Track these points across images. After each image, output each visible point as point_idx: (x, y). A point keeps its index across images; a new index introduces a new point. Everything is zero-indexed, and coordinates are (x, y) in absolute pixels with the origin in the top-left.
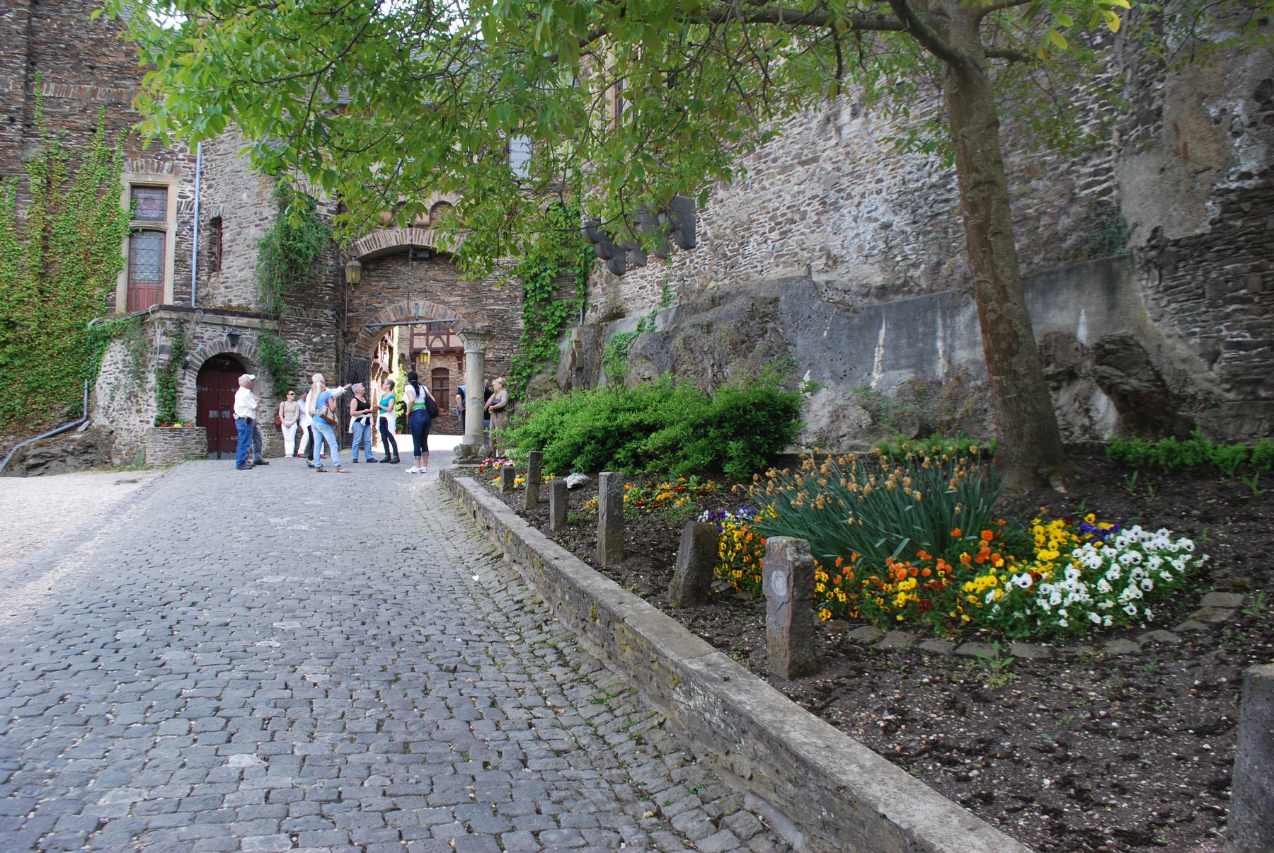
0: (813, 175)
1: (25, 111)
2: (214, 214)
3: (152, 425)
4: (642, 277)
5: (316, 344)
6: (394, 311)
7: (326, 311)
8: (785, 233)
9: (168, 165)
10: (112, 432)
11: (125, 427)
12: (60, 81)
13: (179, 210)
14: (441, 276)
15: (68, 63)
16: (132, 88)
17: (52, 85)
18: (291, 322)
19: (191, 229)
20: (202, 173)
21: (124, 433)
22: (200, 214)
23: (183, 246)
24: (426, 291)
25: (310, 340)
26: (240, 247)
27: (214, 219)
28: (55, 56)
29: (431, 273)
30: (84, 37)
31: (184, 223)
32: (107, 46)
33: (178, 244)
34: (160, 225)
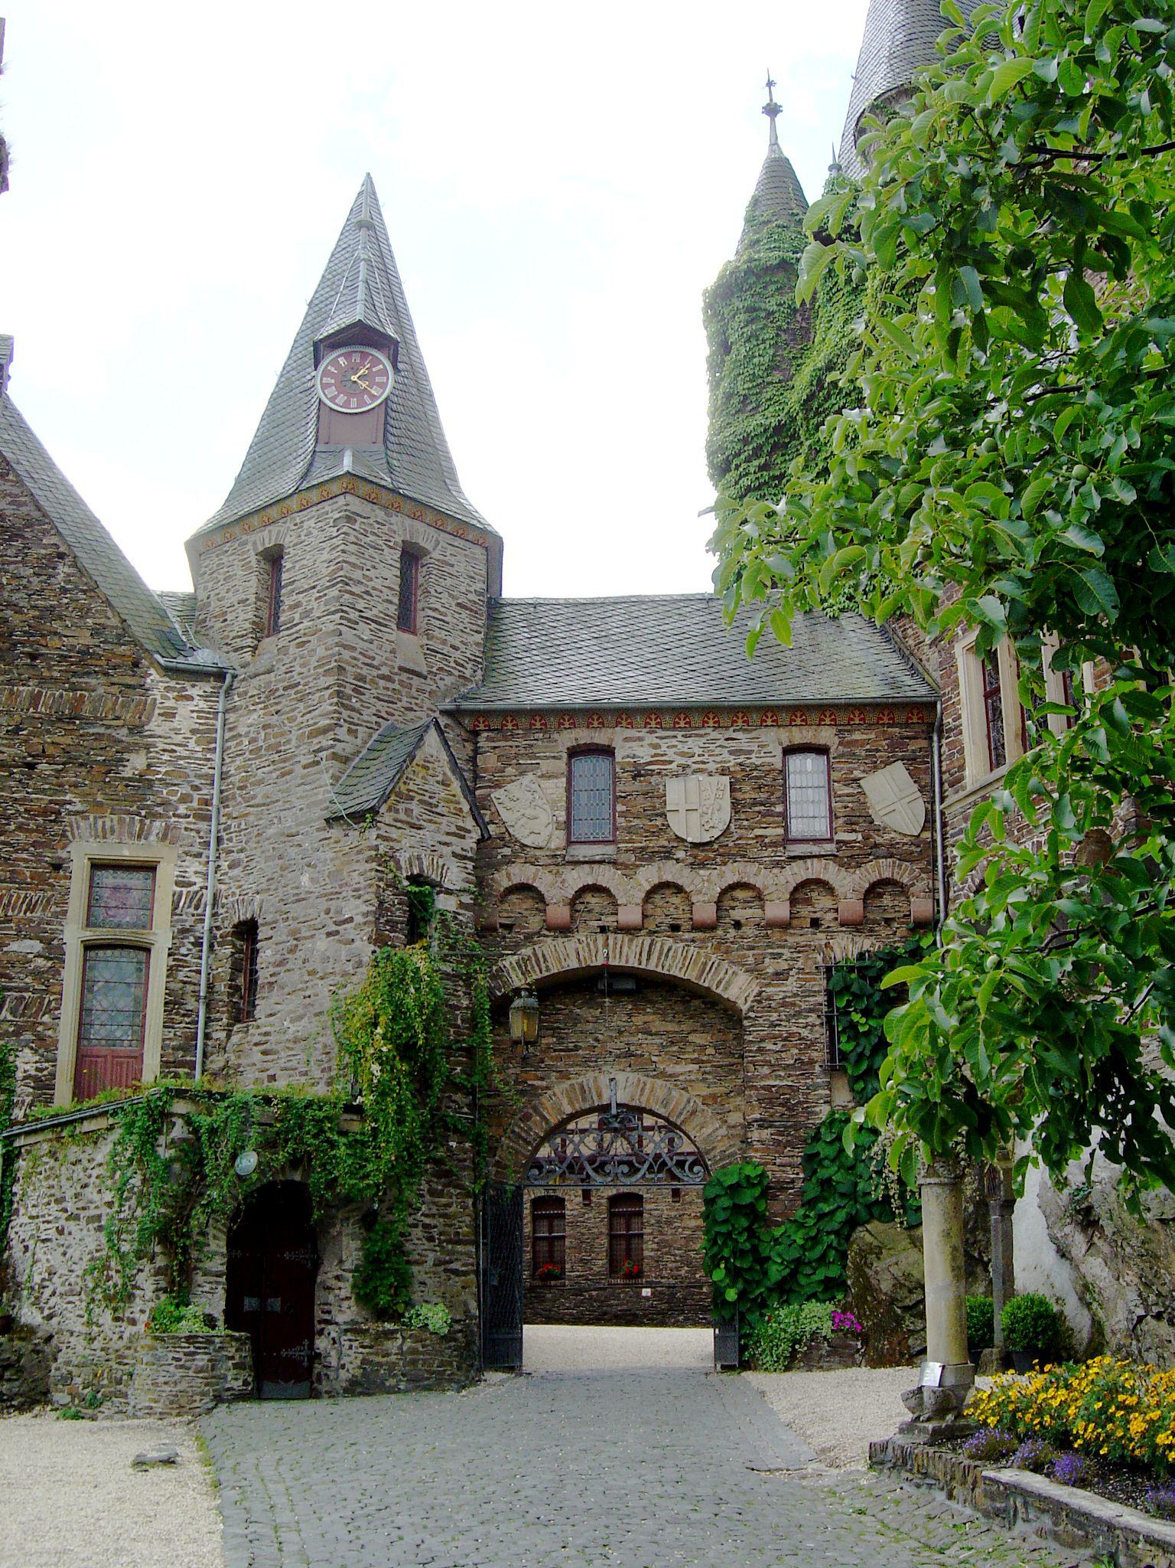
6: (570, 1094)
9: (158, 825)
14: (657, 1025)
16: (101, 690)
19: (198, 944)
20: (219, 840)
24: (629, 1054)
26: (295, 976)
27: (241, 924)
29: (639, 1020)
31: (184, 931)
32: (60, 618)
33: (171, 971)
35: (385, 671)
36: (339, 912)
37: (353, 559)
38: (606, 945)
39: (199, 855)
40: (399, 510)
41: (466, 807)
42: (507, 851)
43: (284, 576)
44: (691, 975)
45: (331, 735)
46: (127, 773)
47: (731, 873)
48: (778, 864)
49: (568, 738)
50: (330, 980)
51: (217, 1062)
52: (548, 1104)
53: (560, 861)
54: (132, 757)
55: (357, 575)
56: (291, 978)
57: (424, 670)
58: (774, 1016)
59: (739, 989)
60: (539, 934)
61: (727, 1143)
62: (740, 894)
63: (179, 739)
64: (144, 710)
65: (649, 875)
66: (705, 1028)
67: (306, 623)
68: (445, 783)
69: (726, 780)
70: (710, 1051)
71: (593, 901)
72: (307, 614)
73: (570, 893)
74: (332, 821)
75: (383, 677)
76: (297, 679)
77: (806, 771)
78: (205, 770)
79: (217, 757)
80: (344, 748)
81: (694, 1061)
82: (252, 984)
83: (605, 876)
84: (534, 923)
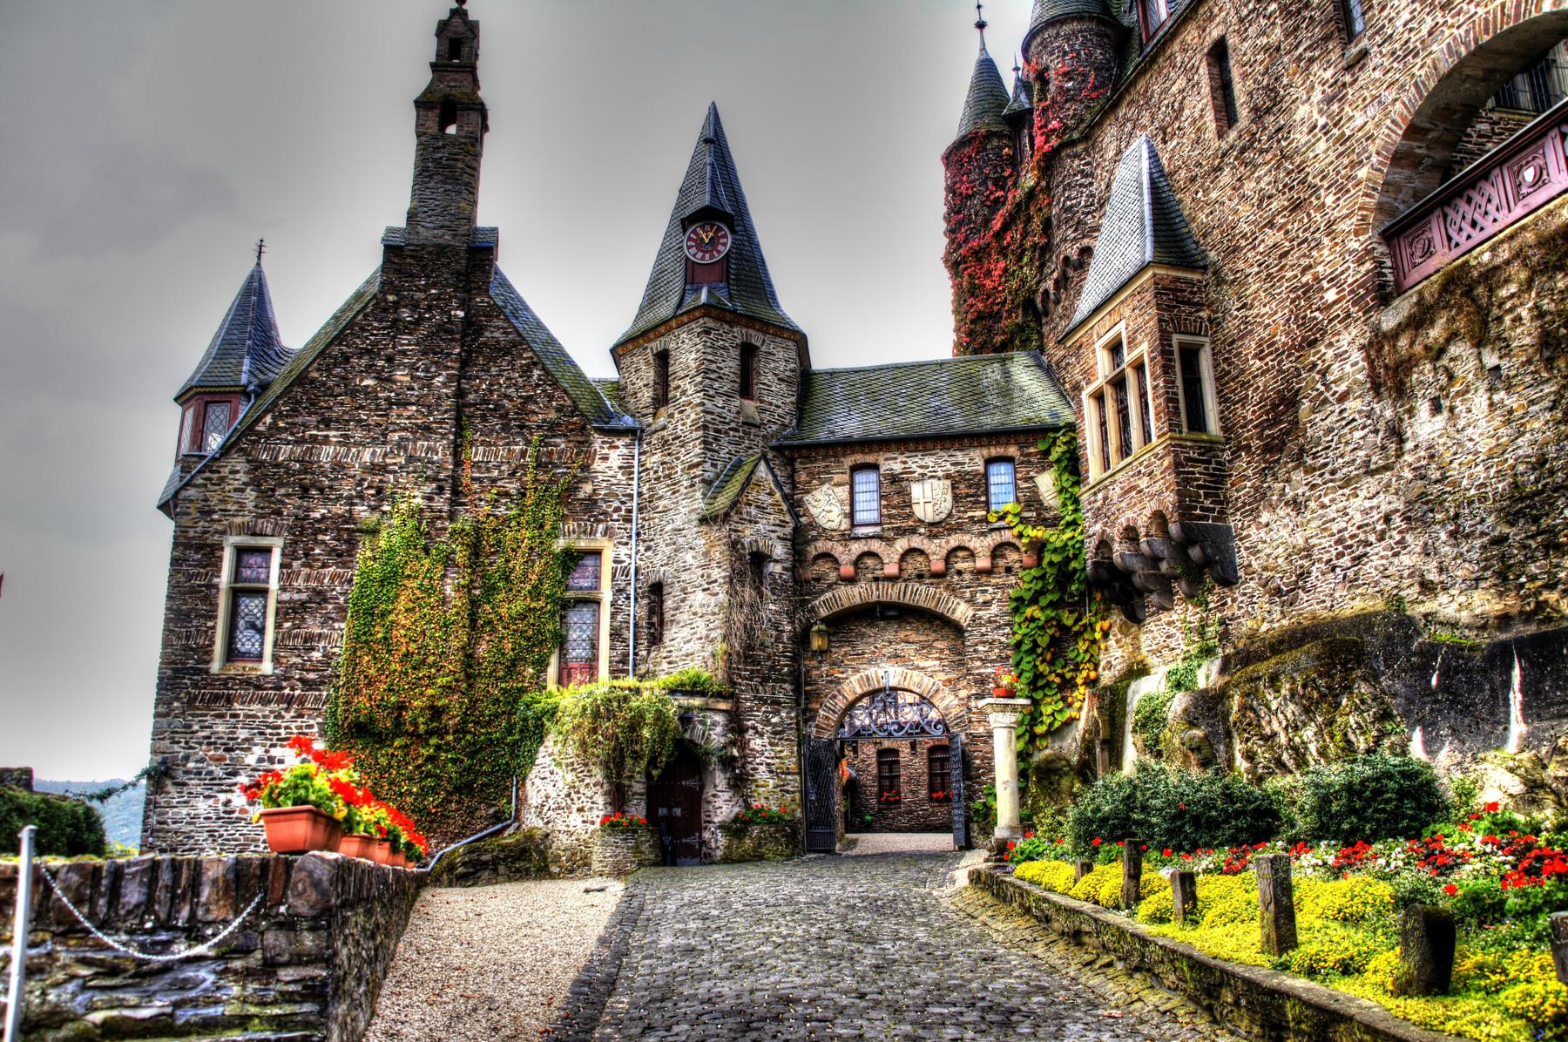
0: (1388, 485)
1: (453, 478)
2: (653, 579)
3: (598, 826)
4: (1169, 624)
5: (775, 725)
7: (785, 686)
8: (1359, 558)
9: (601, 527)
10: (547, 835)
11: (563, 828)
12: (489, 445)
13: (614, 575)
14: (914, 637)
15: (495, 423)
16: (563, 446)
17: (481, 449)
18: (746, 700)
19: (628, 598)
20: (638, 534)
21: (563, 837)
22: (637, 580)
23: (619, 618)
25: (768, 721)
26: (685, 616)
28: (484, 418)
29: (902, 635)
30: (514, 395)
31: (620, 591)
33: (613, 616)
34: (593, 595)
35: (733, 425)
36: (709, 576)
37: (710, 357)
38: (878, 589)
39: (627, 544)
40: (738, 324)
41: (785, 508)
42: (814, 533)
43: (670, 369)
44: (931, 605)
45: (701, 468)
46: (581, 495)
47: (954, 541)
48: (983, 534)
49: (849, 461)
50: (705, 618)
51: (643, 669)
52: (847, 688)
53: (847, 538)
54: (584, 486)
55: (713, 366)
56: (684, 617)
57: (758, 421)
58: (984, 629)
59: (962, 612)
60: (836, 583)
61: (958, 709)
62: (961, 554)
63: (611, 473)
64: (590, 456)
65: (901, 544)
66: (943, 638)
67: (684, 398)
68: (771, 494)
69: (948, 482)
70: (947, 652)
71: (870, 562)
72: (684, 393)
73: (854, 557)
74: (703, 521)
75: (731, 429)
76: (680, 433)
77: (1001, 476)
78: (628, 491)
79: (635, 482)
80: (709, 475)
81: (936, 659)
82: (662, 622)
83: (875, 546)
84: (833, 576)
